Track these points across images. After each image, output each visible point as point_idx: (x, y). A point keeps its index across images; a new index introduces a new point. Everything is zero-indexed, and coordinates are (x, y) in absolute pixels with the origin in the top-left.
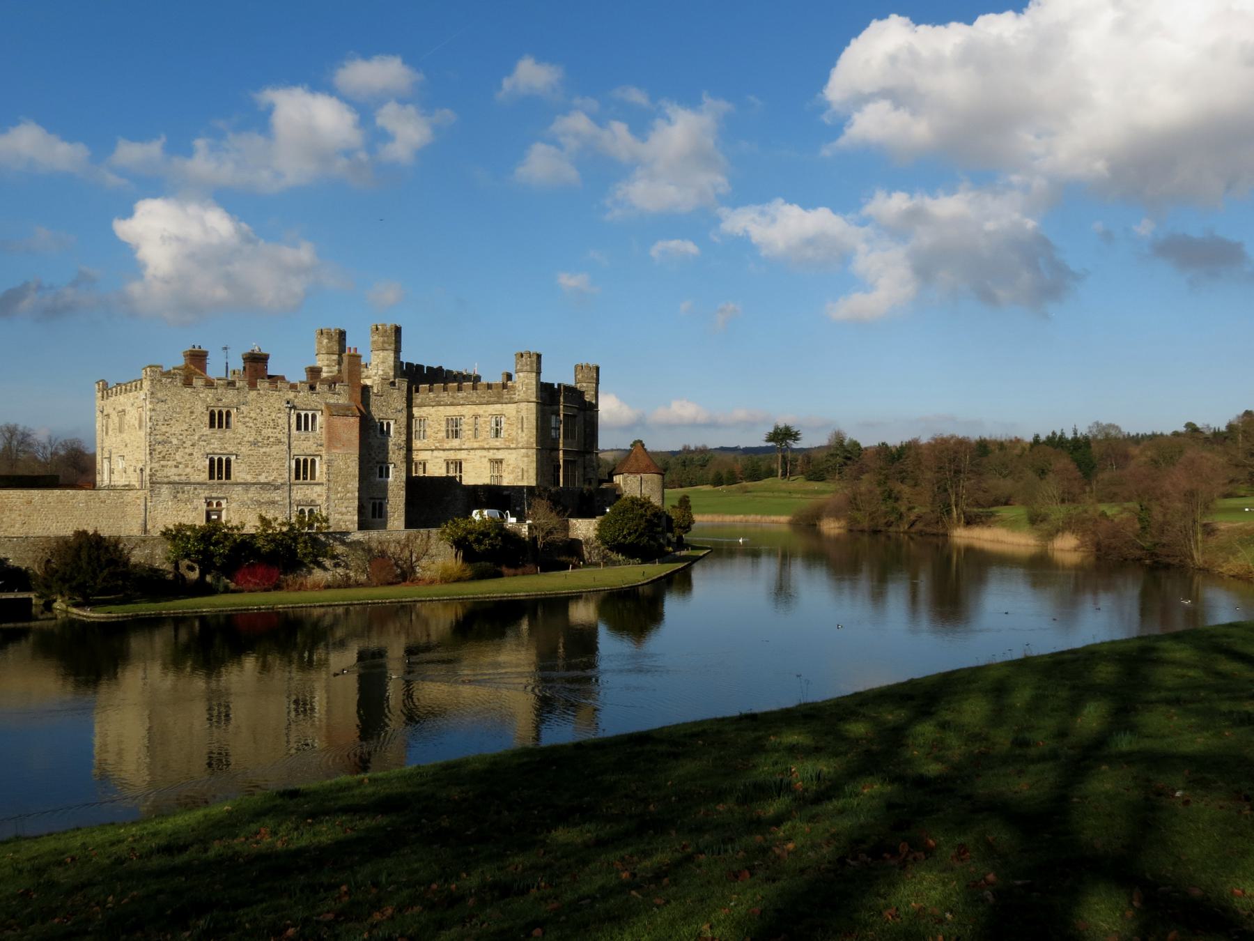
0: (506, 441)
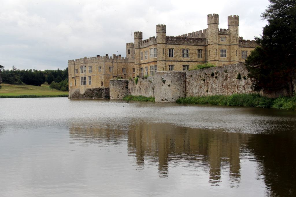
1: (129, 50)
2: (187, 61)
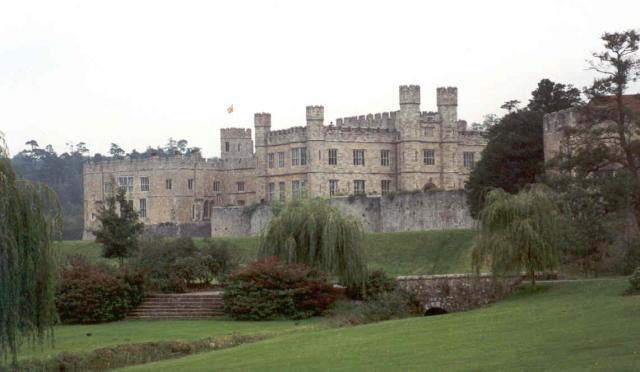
1: (227, 144)
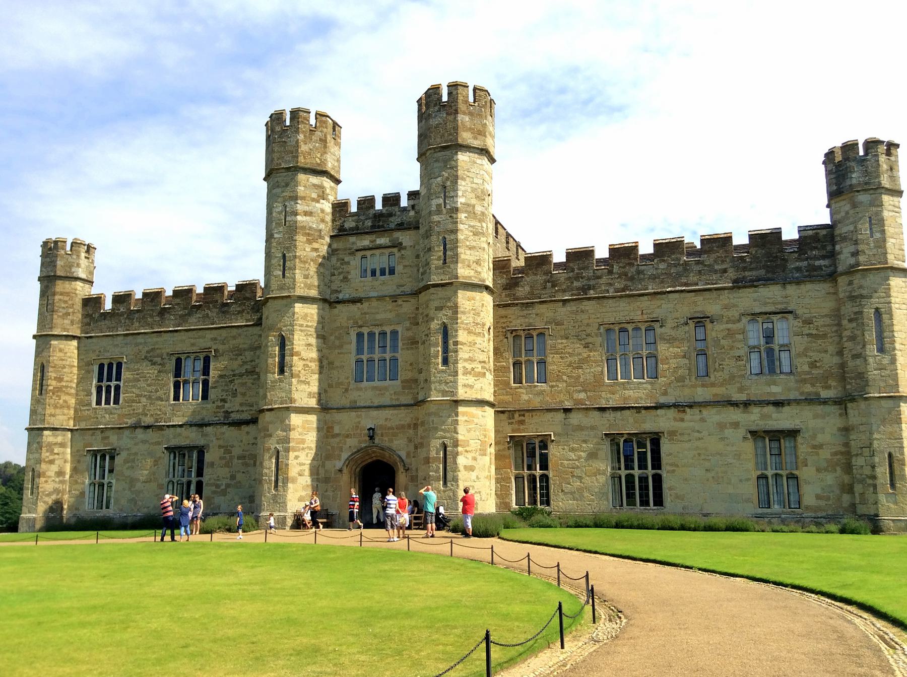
0: (804, 381)
2: (191, 425)
